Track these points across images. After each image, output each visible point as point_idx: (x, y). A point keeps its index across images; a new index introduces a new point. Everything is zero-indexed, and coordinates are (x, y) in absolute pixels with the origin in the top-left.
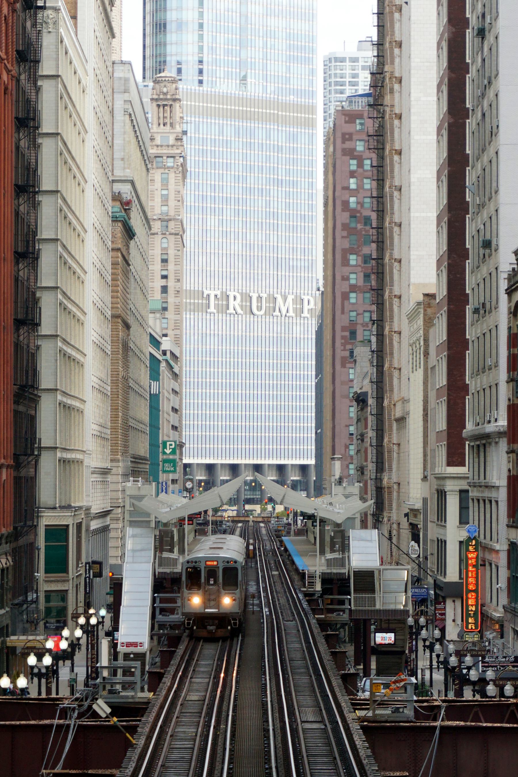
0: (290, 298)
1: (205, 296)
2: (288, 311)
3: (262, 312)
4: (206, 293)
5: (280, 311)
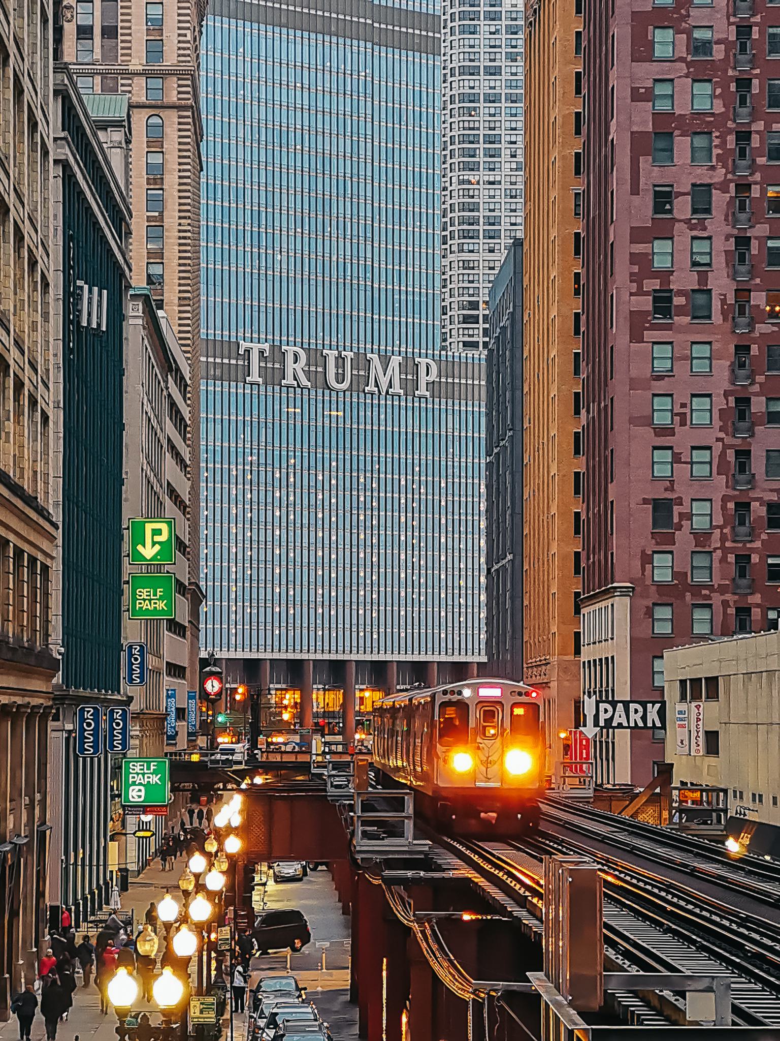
0: (396, 360)
1: (241, 352)
3: (345, 385)
4: (244, 345)
5: (377, 385)
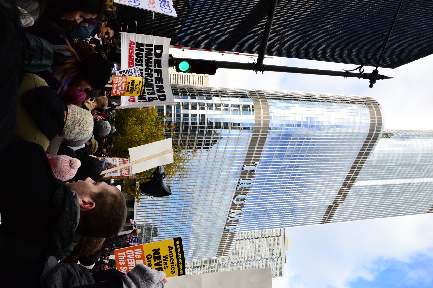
2: (231, 217)
3: (235, 202)
5: (232, 213)
